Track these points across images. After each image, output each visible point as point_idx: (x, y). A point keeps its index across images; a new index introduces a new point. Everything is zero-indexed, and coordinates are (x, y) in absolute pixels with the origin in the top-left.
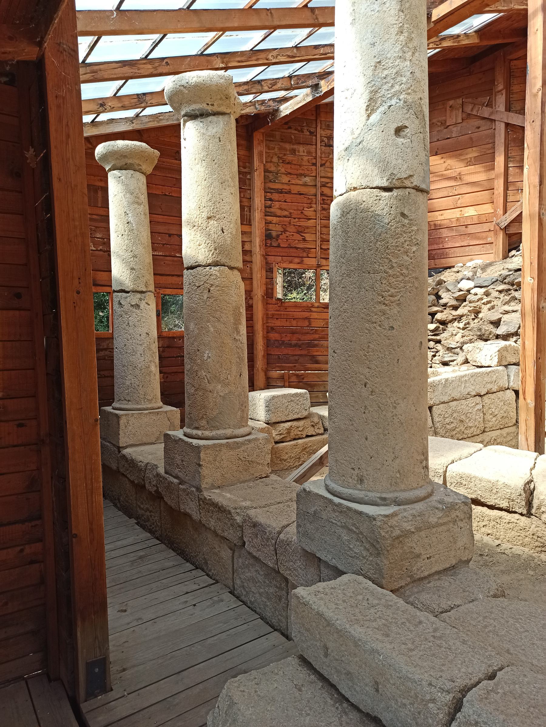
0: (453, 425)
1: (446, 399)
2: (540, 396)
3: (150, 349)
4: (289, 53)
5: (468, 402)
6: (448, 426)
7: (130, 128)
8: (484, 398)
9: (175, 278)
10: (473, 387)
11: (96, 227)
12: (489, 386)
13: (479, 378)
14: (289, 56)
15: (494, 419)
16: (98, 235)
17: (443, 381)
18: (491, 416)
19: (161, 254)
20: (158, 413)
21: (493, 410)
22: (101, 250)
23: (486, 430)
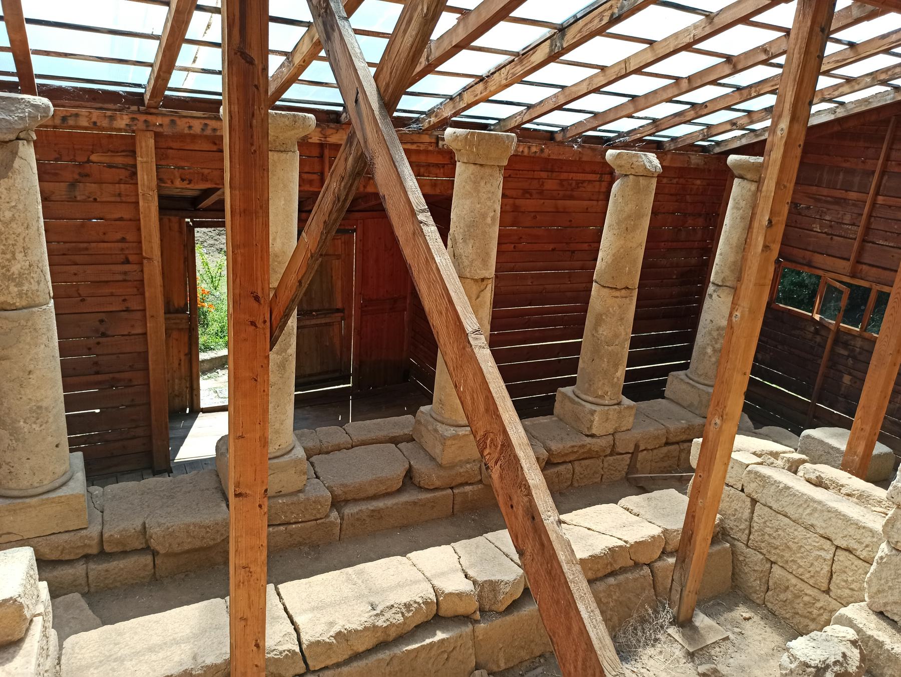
0: (774, 541)
1: (775, 506)
2: (693, 517)
3: (710, 334)
4: (834, 59)
5: (808, 535)
6: (767, 537)
7: (832, 117)
8: (839, 552)
9: (887, 273)
10: (824, 525)
11: (828, 209)
12: (853, 545)
13: (840, 521)
14: (838, 61)
15: (847, 591)
16: (828, 218)
17: (781, 486)
18: (844, 584)
19: (892, 244)
20: (693, 386)
21: (850, 579)
22: (825, 233)
23: (831, 594)
